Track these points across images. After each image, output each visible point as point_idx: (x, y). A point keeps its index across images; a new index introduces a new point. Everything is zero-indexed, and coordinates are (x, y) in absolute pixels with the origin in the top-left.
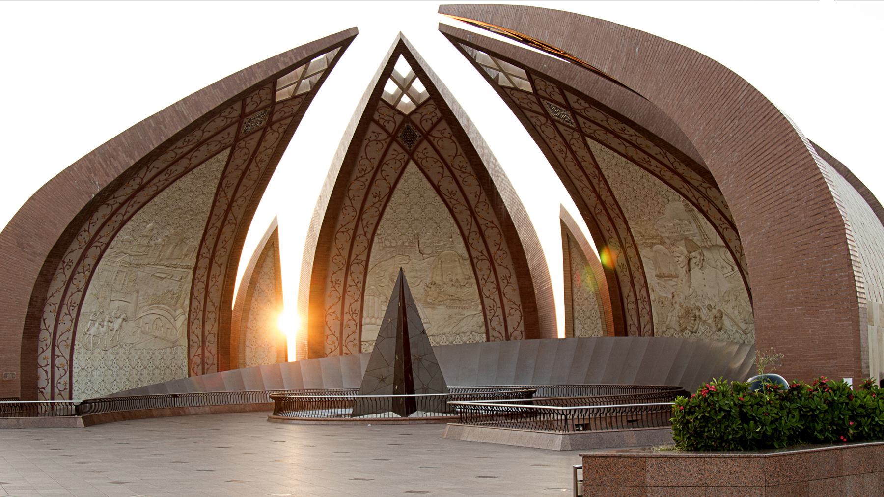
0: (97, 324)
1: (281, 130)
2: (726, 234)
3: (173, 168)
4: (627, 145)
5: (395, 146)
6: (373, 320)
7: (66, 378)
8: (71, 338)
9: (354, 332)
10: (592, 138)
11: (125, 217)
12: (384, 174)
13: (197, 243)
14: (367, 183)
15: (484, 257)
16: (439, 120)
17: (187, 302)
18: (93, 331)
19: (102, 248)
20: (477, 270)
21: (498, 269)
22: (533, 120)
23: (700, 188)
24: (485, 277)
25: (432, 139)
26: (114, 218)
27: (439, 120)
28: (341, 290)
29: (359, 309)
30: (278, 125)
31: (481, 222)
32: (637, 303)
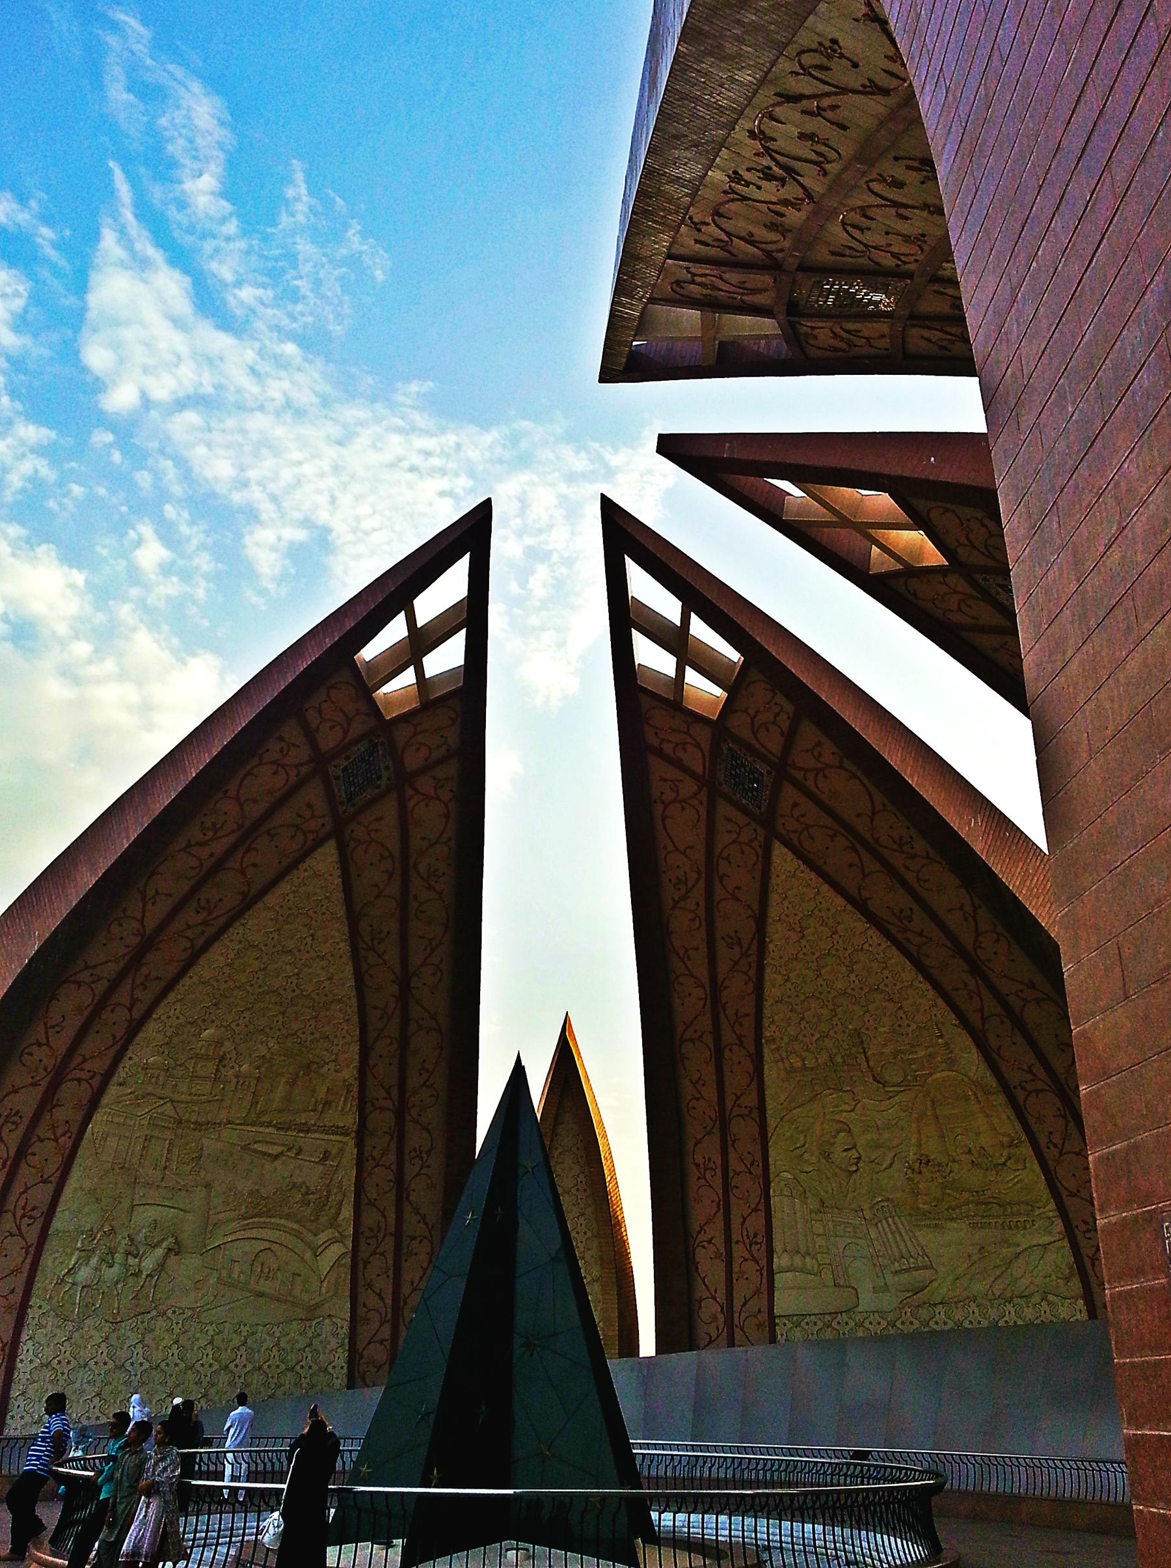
0: (94, 1261)
1: (446, 795)
5: (724, 809)
6: (798, 1260)
8: (19, 1292)
9: (757, 1292)
11: (136, 1014)
13: (349, 1073)
14: (701, 912)
15: (1039, 1085)
17: (347, 1212)
18: (83, 1274)
19: (96, 1082)
20: (1032, 1121)
24: (1056, 1139)
25: (799, 775)
26: (106, 1015)
28: (717, 1182)
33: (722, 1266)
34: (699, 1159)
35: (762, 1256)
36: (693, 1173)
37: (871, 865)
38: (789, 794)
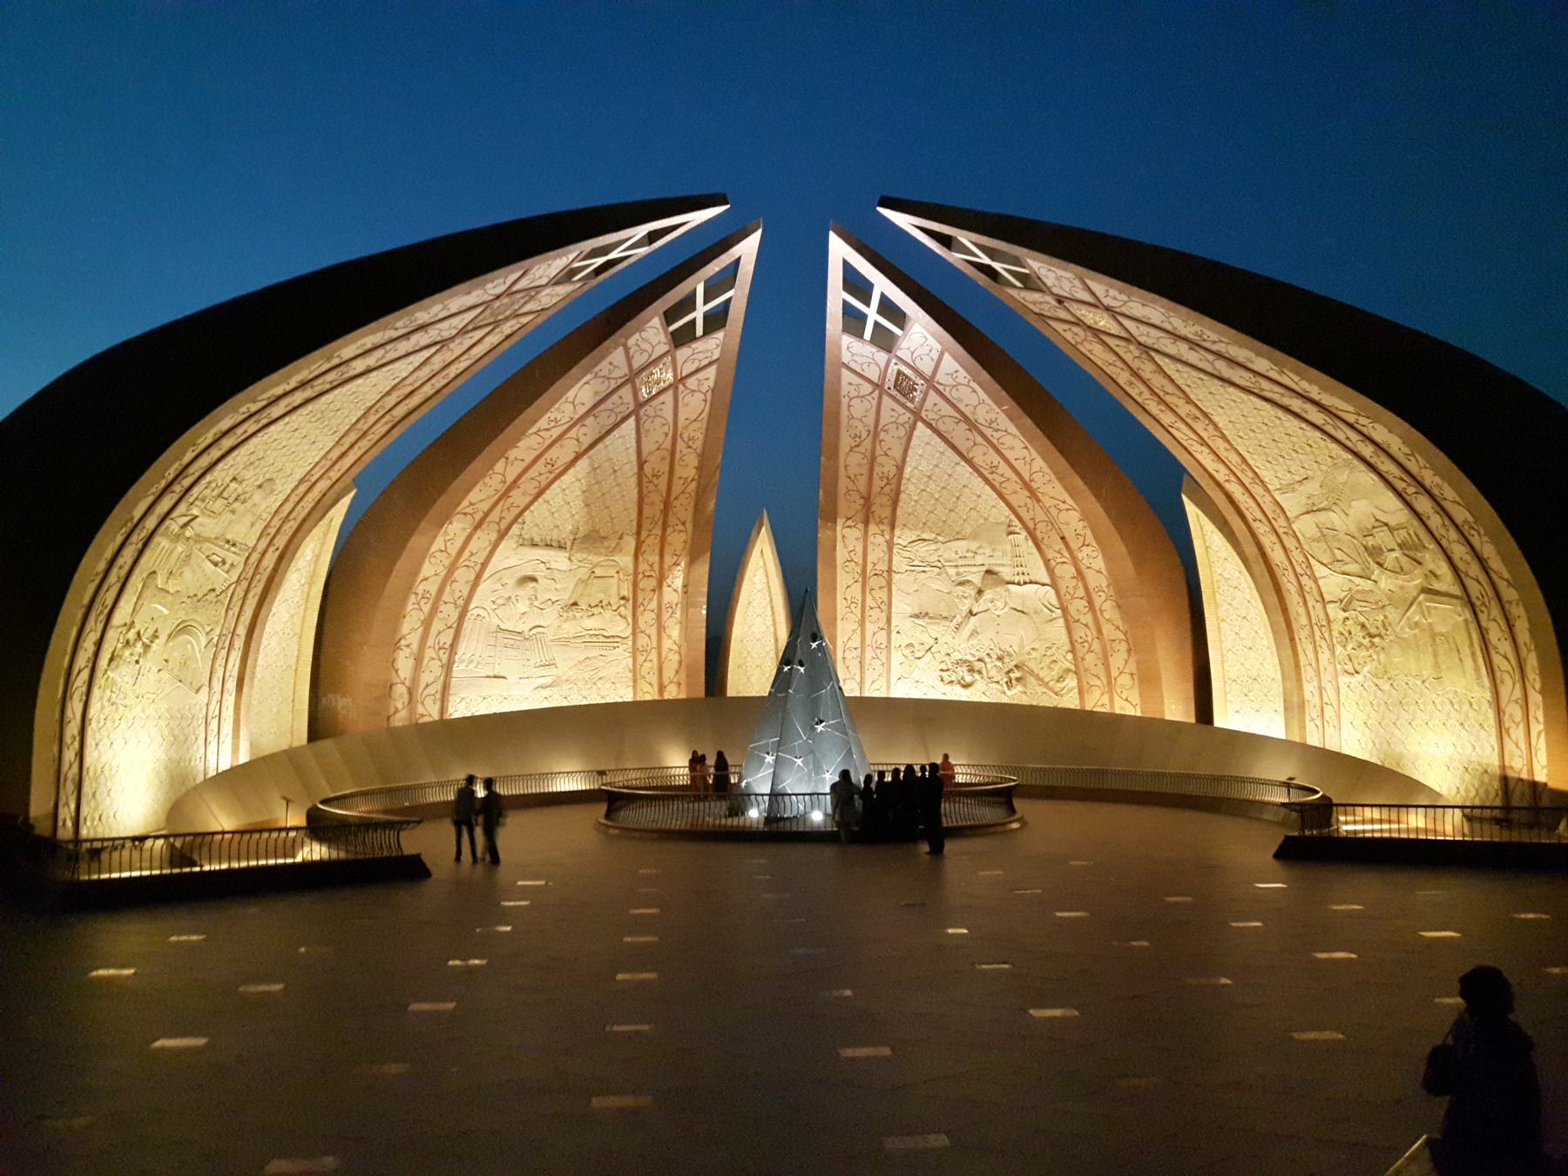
1: (509, 332)
2: (1058, 571)
3: (354, 364)
4: (979, 439)
7: (75, 768)
10: (929, 425)
12: (584, 430)
14: (548, 442)
16: (710, 364)
21: (665, 589)
22: (845, 389)
23: (1052, 510)
27: (710, 364)
28: (426, 608)
29: (449, 642)
30: (513, 322)
31: (672, 520)
32: (863, 651)
33: (411, 661)
34: (420, 591)
35: (445, 659)
36: (412, 599)
37: (668, 444)
38: (668, 397)
